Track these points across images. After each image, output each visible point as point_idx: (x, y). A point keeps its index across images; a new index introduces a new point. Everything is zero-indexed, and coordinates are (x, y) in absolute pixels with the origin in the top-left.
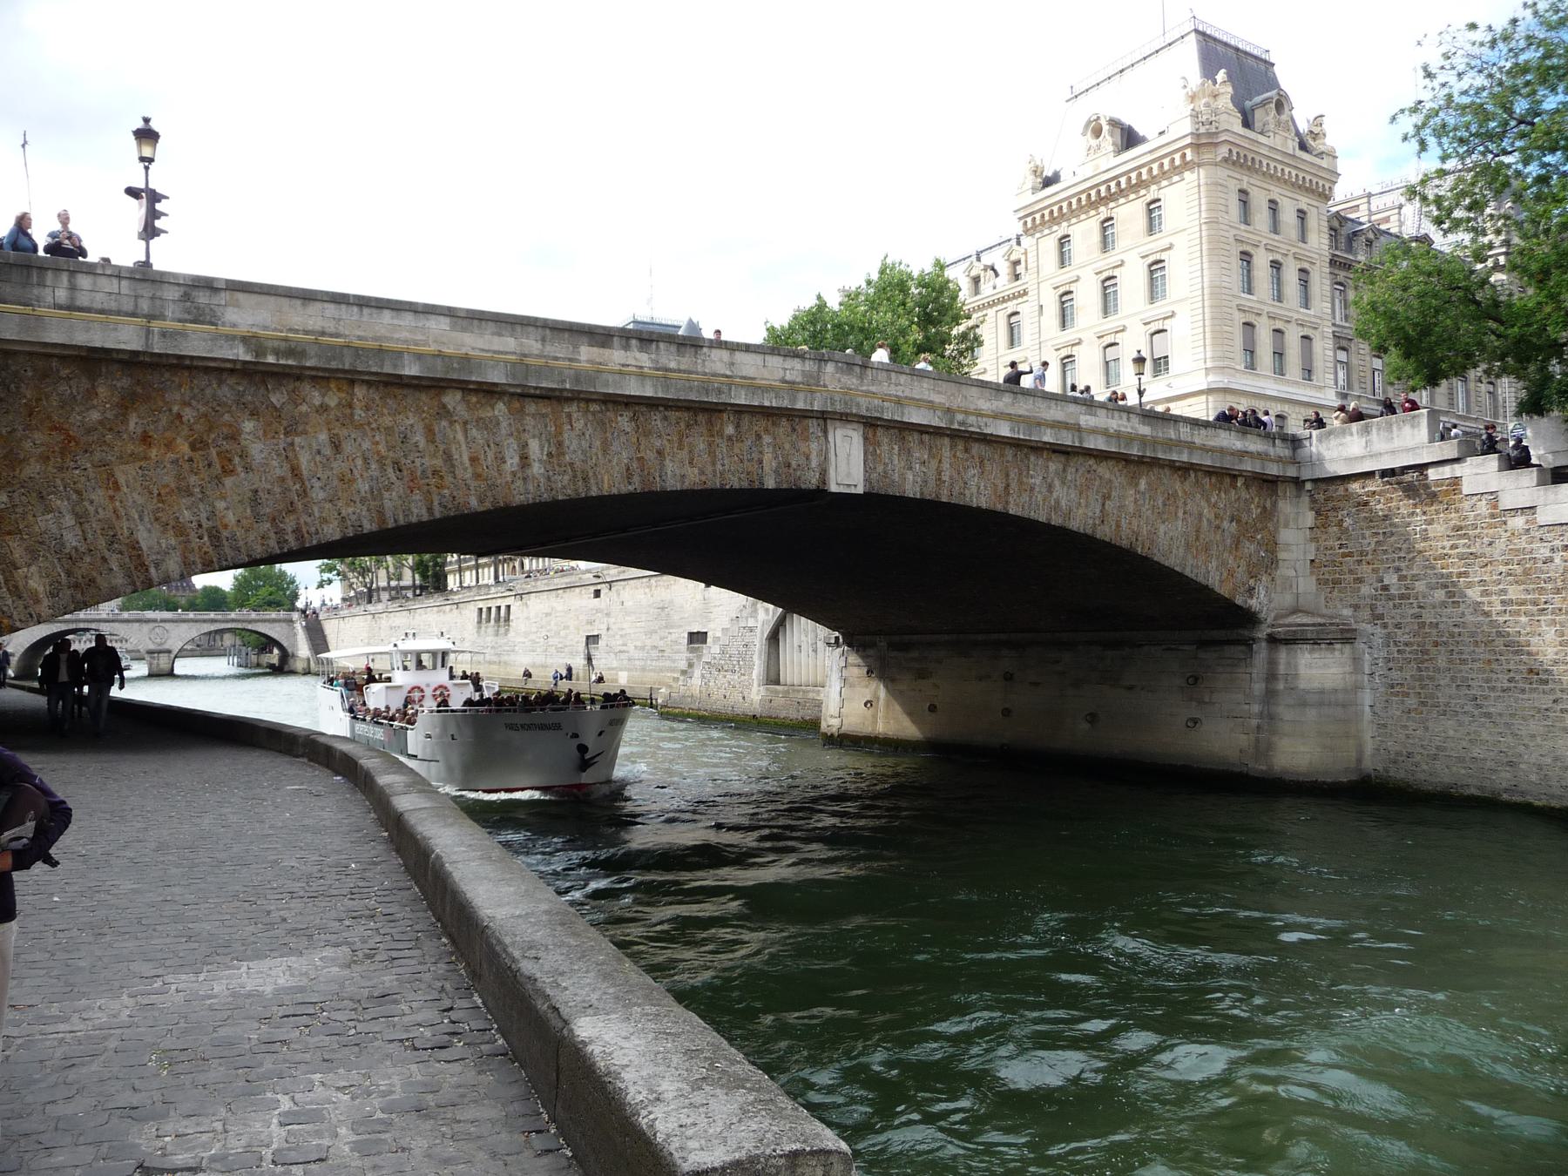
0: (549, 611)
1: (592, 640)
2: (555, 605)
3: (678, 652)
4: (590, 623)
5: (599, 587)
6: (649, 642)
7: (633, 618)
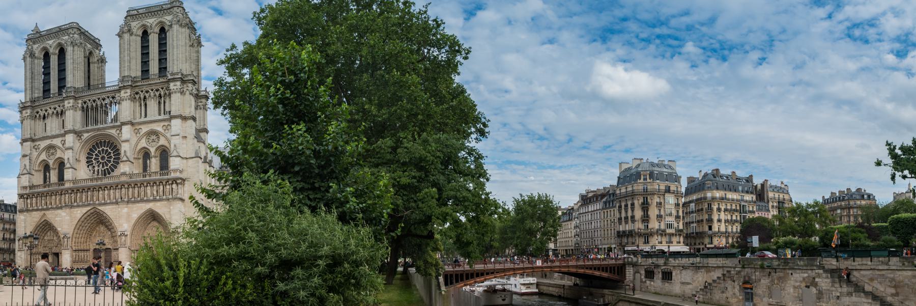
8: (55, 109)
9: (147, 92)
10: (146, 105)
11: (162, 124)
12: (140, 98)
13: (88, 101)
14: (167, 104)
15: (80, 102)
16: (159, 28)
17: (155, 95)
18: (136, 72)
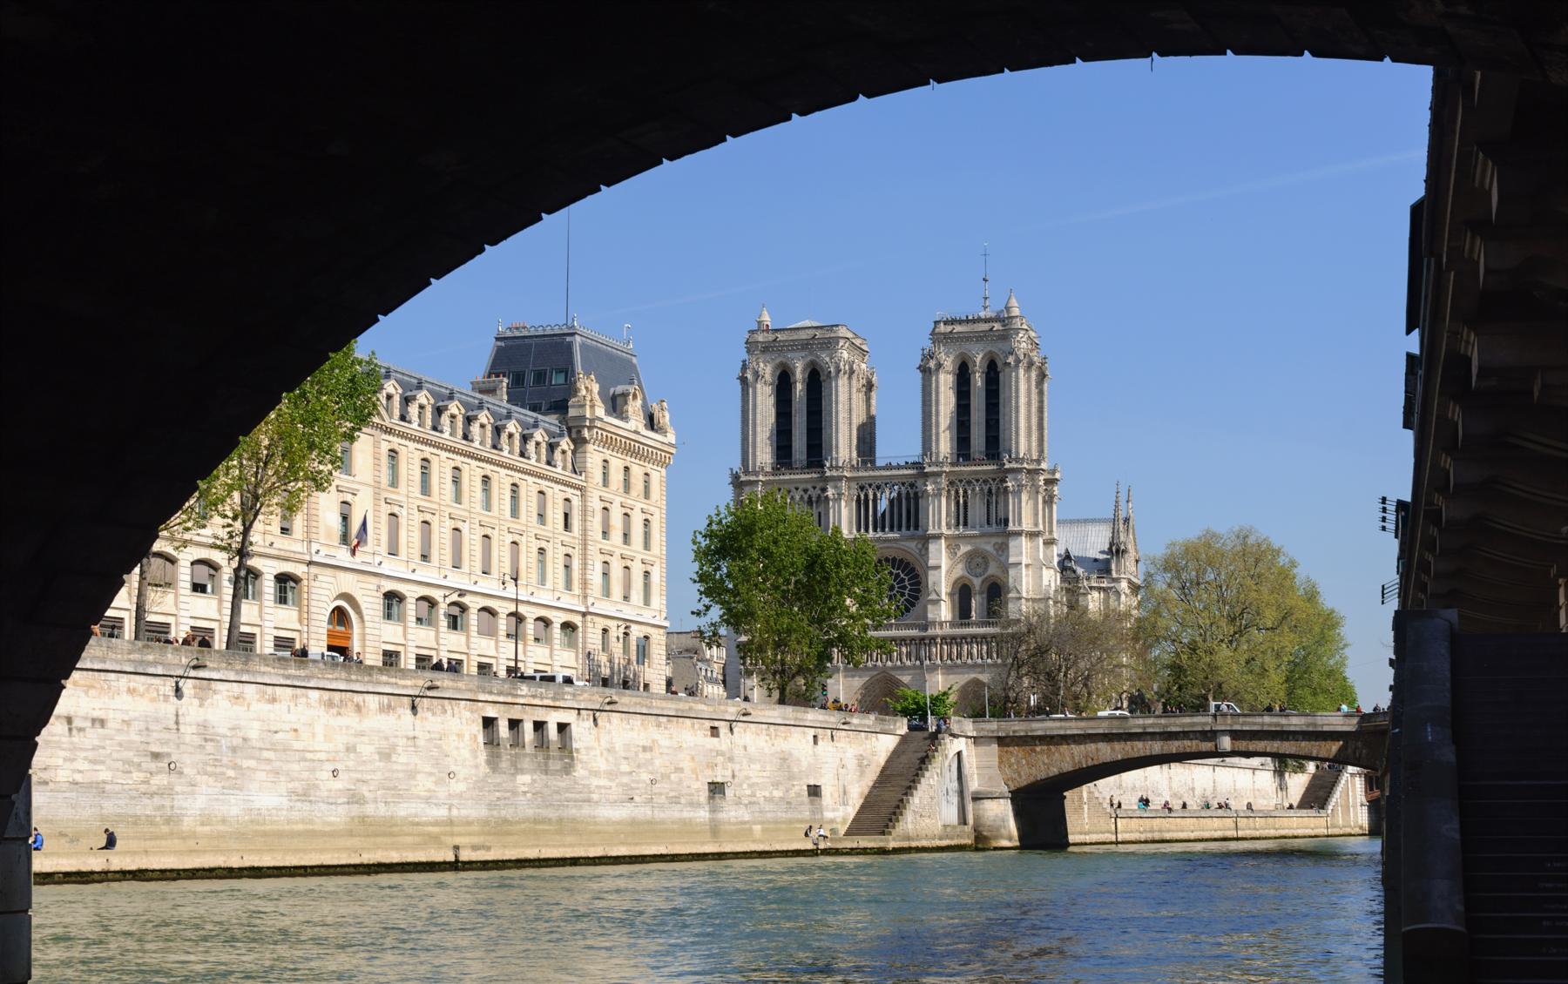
0: (648, 743)
1: (716, 789)
2: (657, 736)
3: (802, 804)
5: (716, 724)
6: (777, 794)
7: (757, 767)
8: (806, 491)
9: (969, 482)
10: (965, 503)
11: (994, 540)
12: (957, 492)
15: (854, 485)
17: (982, 490)
18: (945, 445)
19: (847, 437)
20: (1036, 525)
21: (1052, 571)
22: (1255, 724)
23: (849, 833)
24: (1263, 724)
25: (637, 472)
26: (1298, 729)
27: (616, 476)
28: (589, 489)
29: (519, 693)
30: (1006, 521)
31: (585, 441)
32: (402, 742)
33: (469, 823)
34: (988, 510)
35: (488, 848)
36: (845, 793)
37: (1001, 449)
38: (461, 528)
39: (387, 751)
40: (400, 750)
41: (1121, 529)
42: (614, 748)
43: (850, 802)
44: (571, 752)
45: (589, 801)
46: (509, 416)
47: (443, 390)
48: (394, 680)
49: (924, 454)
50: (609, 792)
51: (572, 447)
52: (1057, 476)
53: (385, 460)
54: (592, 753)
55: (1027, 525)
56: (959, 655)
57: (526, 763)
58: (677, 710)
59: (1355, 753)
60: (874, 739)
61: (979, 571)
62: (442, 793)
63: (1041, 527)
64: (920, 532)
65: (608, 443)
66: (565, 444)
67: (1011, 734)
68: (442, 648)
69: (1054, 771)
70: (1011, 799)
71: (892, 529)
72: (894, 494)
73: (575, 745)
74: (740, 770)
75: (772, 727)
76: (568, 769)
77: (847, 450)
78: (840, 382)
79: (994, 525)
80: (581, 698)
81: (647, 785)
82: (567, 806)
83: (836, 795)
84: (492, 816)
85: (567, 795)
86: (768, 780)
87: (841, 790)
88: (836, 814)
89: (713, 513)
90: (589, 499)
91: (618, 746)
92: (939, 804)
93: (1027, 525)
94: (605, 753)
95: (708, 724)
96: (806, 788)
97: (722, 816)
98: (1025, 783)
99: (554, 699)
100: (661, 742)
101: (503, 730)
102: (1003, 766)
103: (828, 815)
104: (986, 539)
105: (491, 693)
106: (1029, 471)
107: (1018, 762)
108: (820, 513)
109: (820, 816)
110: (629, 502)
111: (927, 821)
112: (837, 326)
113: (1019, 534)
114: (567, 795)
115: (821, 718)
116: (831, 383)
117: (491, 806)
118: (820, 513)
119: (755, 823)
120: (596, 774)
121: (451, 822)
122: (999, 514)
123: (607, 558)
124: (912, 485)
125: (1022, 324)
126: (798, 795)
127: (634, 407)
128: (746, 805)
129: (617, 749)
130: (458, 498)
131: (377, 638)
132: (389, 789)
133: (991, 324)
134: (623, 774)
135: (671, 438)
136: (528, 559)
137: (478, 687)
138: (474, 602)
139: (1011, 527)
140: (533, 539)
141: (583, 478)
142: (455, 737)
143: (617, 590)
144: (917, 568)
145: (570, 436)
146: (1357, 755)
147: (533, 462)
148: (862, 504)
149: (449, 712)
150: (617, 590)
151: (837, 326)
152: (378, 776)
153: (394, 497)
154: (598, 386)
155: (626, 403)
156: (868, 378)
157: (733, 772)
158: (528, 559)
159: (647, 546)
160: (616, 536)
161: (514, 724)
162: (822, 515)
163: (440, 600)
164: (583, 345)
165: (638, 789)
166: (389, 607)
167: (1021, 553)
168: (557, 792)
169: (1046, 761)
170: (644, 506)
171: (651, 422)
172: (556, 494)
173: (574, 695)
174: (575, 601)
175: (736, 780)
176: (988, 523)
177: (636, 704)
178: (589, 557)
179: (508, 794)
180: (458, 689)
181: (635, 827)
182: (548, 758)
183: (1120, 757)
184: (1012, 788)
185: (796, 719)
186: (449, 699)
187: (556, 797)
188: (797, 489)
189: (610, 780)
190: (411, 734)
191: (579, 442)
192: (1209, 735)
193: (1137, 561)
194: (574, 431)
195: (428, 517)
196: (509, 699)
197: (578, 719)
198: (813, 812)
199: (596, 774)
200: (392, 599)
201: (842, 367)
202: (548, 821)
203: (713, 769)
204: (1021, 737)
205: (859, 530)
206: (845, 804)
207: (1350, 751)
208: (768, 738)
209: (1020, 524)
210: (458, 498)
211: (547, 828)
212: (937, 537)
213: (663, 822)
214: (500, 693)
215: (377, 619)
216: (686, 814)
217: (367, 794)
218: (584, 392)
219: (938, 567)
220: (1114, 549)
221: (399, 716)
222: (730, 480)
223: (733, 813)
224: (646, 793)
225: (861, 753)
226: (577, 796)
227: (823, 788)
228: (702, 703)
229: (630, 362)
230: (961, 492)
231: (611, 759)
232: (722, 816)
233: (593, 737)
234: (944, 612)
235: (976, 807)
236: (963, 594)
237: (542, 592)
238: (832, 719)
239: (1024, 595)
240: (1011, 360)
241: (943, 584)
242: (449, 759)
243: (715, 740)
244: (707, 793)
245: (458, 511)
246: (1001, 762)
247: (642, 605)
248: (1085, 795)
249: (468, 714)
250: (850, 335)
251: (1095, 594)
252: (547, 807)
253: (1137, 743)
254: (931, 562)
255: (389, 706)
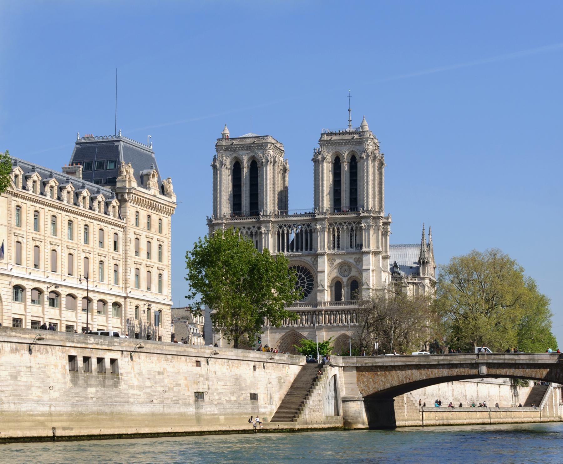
0: (161, 370)
1: (199, 395)
3: (247, 404)
4: (197, 383)
5: (199, 359)
6: (233, 398)
7: (222, 383)
8: (249, 229)
9: (340, 224)
11: (354, 256)
12: (334, 230)
13: (283, 226)
14: (358, 237)
15: (276, 225)
16: (351, 157)
17: (347, 228)
19: (272, 199)
20: (378, 248)
21: (387, 274)
22: (500, 359)
23: (273, 421)
24: (505, 359)
25: (155, 218)
26: (524, 362)
27: (143, 221)
28: (128, 228)
29: (89, 342)
30: (361, 246)
31: (126, 201)
32: (24, 369)
33: (61, 415)
34: (351, 240)
35: (72, 429)
36: (271, 398)
37: (358, 205)
38: (56, 250)
39: (15, 374)
40: (22, 374)
41: (425, 250)
42: (142, 372)
43: (274, 403)
44: (118, 375)
45: (128, 402)
46: (83, 187)
47: (47, 172)
48: (19, 335)
49: (315, 208)
50: (139, 397)
51: (119, 204)
52: (390, 220)
53: (14, 211)
54: (130, 375)
55: (373, 248)
56: (335, 321)
57: (93, 381)
58: (177, 351)
59: (556, 375)
60: (287, 368)
61: (346, 273)
62: (46, 398)
63: (381, 249)
64: (313, 252)
65: (138, 202)
66: (115, 202)
67: (364, 365)
68: (46, 316)
69: (388, 386)
70: (364, 401)
71: (297, 250)
72: (299, 231)
73: (120, 371)
74: (213, 385)
75: (230, 361)
76: (116, 384)
77: (272, 206)
78: (268, 168)
79: (355, 248)
80: (124, 345)
81: (160, 393)
82: (116, 405)
83: (266, 399)
84: (74, 411)
85: (116, 399)
86: (228, 391)
87: (269, 396)
88: (266, 410)
89: (197, 241)
90: (128, 233)
91: (145, 372)
92: (323, 404)
93: (373, 248)
94: (137, 375)
95: (194, 359)
96: (249, 395)
97: (202, 411)
98: (372, 392)
99: (108, 345)
100: (168, 370)
101: (80, 362)
102: (359, 383)
103: (262, 410)
104: (350, 256)
105: (73, 342)
106: (374, 218)
107: (368, 381)
108: (257, 241)
109: (257, 411)
110: (151, 235)
111: (317, 413)
112: (267, 136)
113: (368, 253)
114: (116, 399)
115: (258, 356)
116: (263, 168)
117: (73, 405)
118: (257, 241)
119: (221, 415)
120: (132, 387)
121: (51, 414)
122: (357, 241)
123: (138, 266)
124: (308, 226)
125: (370, 135)
126: (245, 399)
127: (153, 182)
128: (216, 405)
129: (143, 373)
130: (55, 233)
131: (9, 311)
132: (16, 396)
133: (353, 135)
134: (146, 387)
135: (174, 199)
136: (94, 267)
137: (66, 339)
138: (64, 292)
139: (364, 249)
140: (97, 256)
141: (125, 221)
142: (53, 367)
143: (144, 284)
144: (312, 272)
145: (117, 198)
146: (558, 377)
147: (97, 212)
148: (280, 236)
149: (50, 352)
150: (144, 284)
151: (267, 136)
152: (10, 388)
153: (19, 232)
154: (133, 170)
155: (149, 179)
156: (284, 165)
157: (209, 386)
158: (94, 267)
159: (160, 259)
160: (143, 254)
161: (86, 359)
162: (258, 242)
163: (45, 290)
164: (124, 147)
165: (155, 396)
166: (16, 294)
167: (370, 264)
168: (110, 398)
169: (384, 380)
170: (159, 237)
171: (163, 190)
172: (109, 230)
173: (120, 343)
174: (121, 291)
175: (210, 391)
176: (351, 247)
177: (154, 348)
178: (128, 266)
179: (83, 399)
180: (55, 340)
181: (154, 417)
182: (105, 378)
183: (425, 378)
184: (365, 395)
185: (244, 356)
186: (50, 345)
187: (110, 400)
188: (244, 228)
189: (140, 391)
190: (29, 365)
191: (122, 201)
192: (475, 365)
193: (434, 268)
194: (119, 195)
195: (38, 243)
196: (84, 346)
197: (122, 357)
198: (253, 409)
199: (132, 387)
200: (18, 289)
201: (269, 159)
202: (105, 414)
203: (197, 385)
204: (369, 366)
205: (279, 250)
206: (271, 404)
207: (553, 374)
208: (228, 367)
209: (369, 247)
210: (55, 233)
211: (105, 417)
212: (323, 255)
213: (169, 414)
214: (78, 342)
215: (9, 301)
216: (182, 410)
217: (4, 398)
218: (125, 173)
219: (323, 272)
220: (421, 261)
221: (22, 355)
222: (207, 223)
223: (208, 409)
224: (160, 398)
225: (280, 375)
226: (122, 400)
227: (259, 395)
228: (191, 347)
229: (151, 156)
230: (336, 229)
231: (140, 379)
232: (202, 411)
233: (130, 366)
234: (327, 296)
235: (345, 406)
236: (337, 286)
237: (101, 285)
238: (264, 357)
239: (371, 287)
240: (364, 155)
241: (326, 281)
242: (50, 379)
243: (199, 368)
244: (194, 398)
245: (55, 240)
246: (358, 381)
247: (157, 292)
248: (405, 399)
249: (60, 354)
250: (274, 141)
251: (411, 287)
252: (104, 406)
253: (434, 370)
254: (319, 269)
255: (16, 349)
